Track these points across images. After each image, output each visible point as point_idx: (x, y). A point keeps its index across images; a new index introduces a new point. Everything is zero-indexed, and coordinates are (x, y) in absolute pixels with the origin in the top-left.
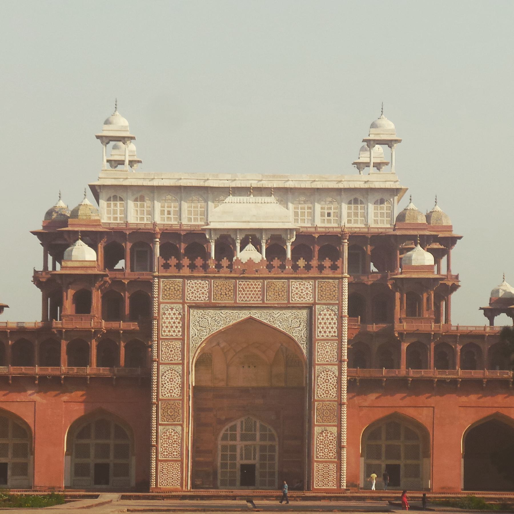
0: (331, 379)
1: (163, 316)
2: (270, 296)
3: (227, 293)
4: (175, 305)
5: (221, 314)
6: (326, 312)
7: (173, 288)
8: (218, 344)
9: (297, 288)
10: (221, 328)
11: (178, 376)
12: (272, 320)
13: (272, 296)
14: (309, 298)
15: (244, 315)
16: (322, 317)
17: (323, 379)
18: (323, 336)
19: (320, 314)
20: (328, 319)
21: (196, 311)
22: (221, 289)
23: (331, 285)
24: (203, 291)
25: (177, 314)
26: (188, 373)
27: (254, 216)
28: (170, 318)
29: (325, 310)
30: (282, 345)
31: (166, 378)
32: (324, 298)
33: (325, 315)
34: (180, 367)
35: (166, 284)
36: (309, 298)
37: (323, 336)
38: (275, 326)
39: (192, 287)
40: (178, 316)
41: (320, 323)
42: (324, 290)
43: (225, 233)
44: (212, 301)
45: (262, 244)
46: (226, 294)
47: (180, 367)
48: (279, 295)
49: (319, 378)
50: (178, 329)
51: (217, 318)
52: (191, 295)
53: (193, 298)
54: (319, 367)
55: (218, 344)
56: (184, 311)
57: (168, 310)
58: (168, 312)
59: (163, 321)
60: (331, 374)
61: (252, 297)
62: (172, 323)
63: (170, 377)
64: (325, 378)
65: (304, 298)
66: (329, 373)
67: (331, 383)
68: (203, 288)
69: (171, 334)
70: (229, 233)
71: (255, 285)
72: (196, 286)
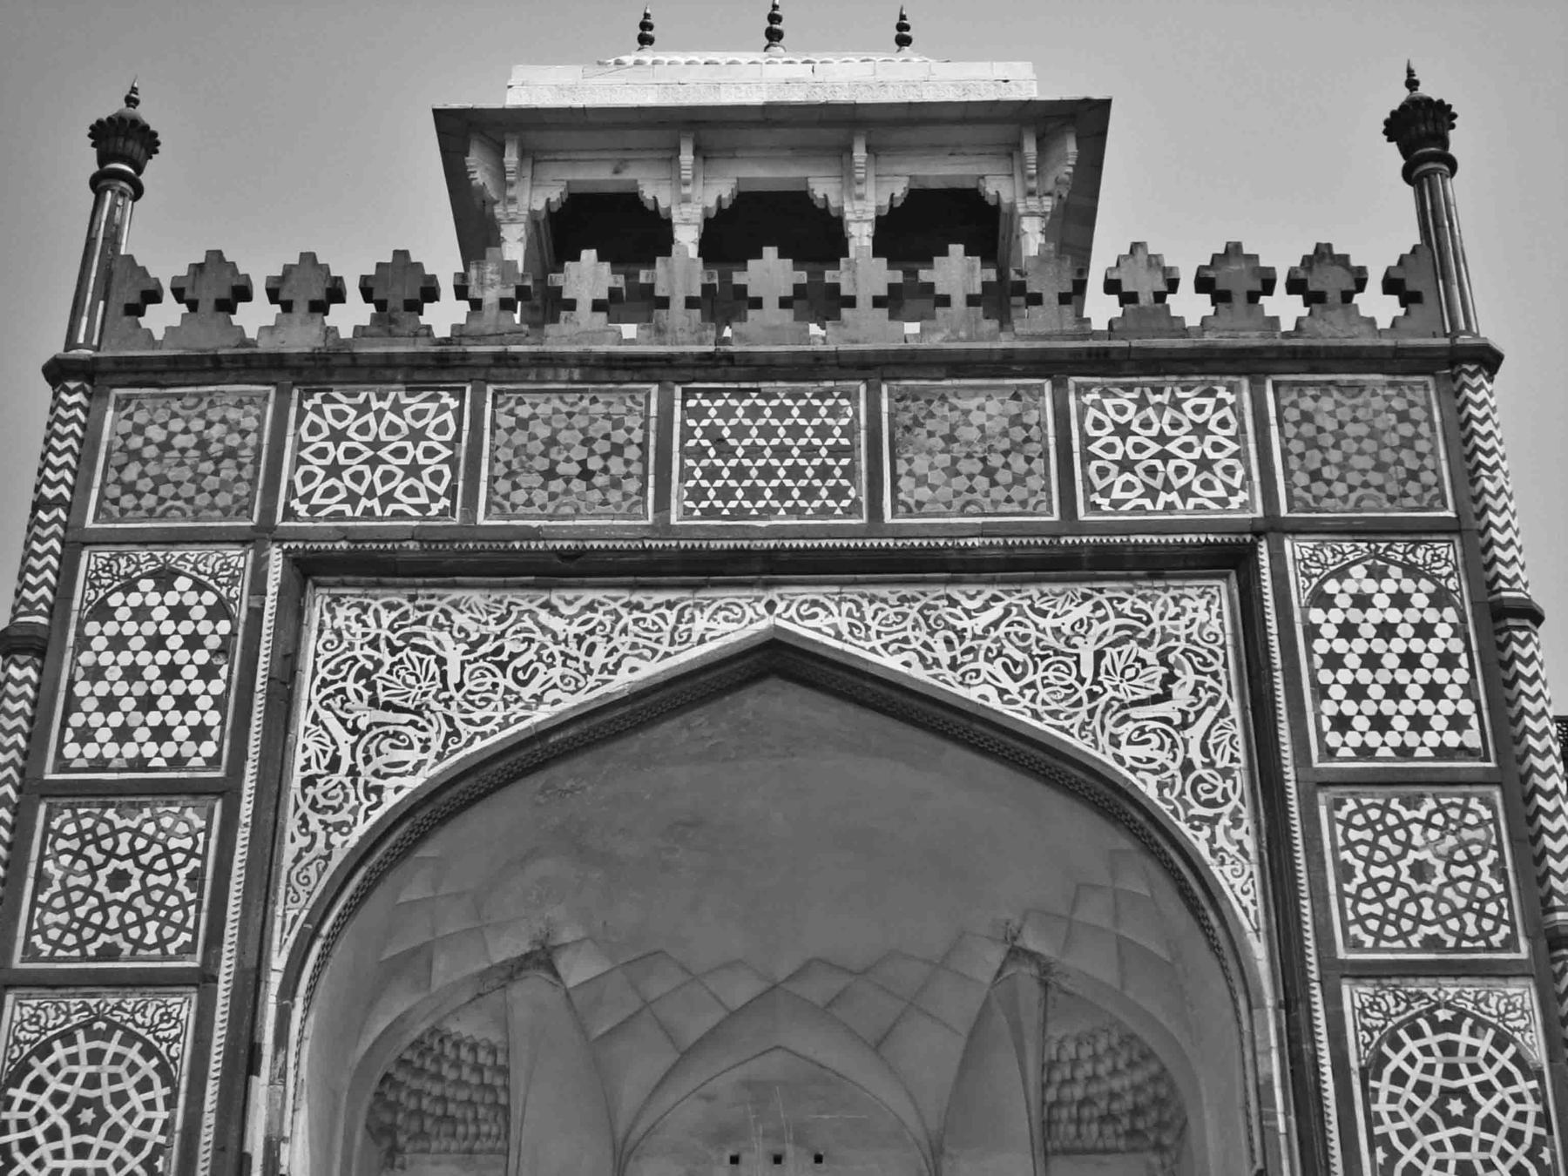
0: (1486, 1089)
1: (92, 628)
2: (921, 481)
3: (595, 464)
4: (193, 553)
5: (544, 616)
6: (1370, 586)
7: (191, 440)
8: (542, 958)
9: (1123, 431)
10: (541, 715)
11: (144, 1085)
12: (945, 656)
13: (935, 477)
14: (1220, 492)
15: (726, 622)
16: (1336, 616)
17: (1422, 1089)
18: (1365, 752)
19: (1323, 600)
20: (1386, 631)
21: (351, 595)
22: (552, 441)
23: (1378, 403)
24: (415, 453)
25: (198, 613)
26: (245, 1059)
27: (798, 81)
28: (137, 643)
29: (1358, 571)
30: (1016, 954)
31: (42, 1100)
32: (1340, 489)
33: (1362, 601)
34: (184, 1007)
35: (141, 417)
36: (1220, 492)
37: (1365, 752)
38: (972, 694)
39: (337, 436)
40: (205, 628)
41: (1334, 661)
42: (1327, 440)
43: (598, 175)
44: (481, 520)
45: (853, 229)
46: (586, 475)
47: (184, 1007)
48: (989, 472)
49: (1384, 1086)
50: (193, 718)
51: (510, 647)
52: (320, 485)
53: (333, 504)
54: (1365, 991)
55: (542, 958)
56: (258, 588)
57: (129, 586)
58: (135, 599)
59: (86, 658)
60: (1484, 1044)
61: (782, 493)
62: (152, 673)
63: (74, 1091)
64: (1437, 1081)
65: (1186, 493)
66: (1464, 1039)
67: (1491, 1125)
68: (417, 436)
69: (130, 750)
70: (629, 175)
71: (809, 412)
72: (363, 429)
